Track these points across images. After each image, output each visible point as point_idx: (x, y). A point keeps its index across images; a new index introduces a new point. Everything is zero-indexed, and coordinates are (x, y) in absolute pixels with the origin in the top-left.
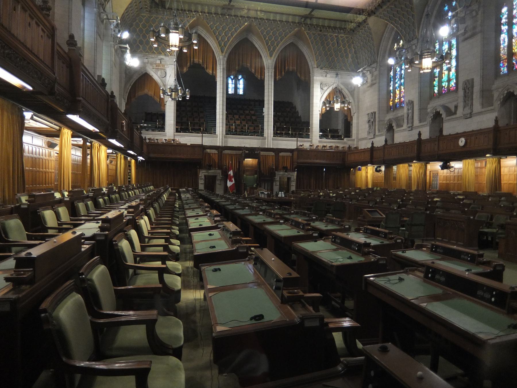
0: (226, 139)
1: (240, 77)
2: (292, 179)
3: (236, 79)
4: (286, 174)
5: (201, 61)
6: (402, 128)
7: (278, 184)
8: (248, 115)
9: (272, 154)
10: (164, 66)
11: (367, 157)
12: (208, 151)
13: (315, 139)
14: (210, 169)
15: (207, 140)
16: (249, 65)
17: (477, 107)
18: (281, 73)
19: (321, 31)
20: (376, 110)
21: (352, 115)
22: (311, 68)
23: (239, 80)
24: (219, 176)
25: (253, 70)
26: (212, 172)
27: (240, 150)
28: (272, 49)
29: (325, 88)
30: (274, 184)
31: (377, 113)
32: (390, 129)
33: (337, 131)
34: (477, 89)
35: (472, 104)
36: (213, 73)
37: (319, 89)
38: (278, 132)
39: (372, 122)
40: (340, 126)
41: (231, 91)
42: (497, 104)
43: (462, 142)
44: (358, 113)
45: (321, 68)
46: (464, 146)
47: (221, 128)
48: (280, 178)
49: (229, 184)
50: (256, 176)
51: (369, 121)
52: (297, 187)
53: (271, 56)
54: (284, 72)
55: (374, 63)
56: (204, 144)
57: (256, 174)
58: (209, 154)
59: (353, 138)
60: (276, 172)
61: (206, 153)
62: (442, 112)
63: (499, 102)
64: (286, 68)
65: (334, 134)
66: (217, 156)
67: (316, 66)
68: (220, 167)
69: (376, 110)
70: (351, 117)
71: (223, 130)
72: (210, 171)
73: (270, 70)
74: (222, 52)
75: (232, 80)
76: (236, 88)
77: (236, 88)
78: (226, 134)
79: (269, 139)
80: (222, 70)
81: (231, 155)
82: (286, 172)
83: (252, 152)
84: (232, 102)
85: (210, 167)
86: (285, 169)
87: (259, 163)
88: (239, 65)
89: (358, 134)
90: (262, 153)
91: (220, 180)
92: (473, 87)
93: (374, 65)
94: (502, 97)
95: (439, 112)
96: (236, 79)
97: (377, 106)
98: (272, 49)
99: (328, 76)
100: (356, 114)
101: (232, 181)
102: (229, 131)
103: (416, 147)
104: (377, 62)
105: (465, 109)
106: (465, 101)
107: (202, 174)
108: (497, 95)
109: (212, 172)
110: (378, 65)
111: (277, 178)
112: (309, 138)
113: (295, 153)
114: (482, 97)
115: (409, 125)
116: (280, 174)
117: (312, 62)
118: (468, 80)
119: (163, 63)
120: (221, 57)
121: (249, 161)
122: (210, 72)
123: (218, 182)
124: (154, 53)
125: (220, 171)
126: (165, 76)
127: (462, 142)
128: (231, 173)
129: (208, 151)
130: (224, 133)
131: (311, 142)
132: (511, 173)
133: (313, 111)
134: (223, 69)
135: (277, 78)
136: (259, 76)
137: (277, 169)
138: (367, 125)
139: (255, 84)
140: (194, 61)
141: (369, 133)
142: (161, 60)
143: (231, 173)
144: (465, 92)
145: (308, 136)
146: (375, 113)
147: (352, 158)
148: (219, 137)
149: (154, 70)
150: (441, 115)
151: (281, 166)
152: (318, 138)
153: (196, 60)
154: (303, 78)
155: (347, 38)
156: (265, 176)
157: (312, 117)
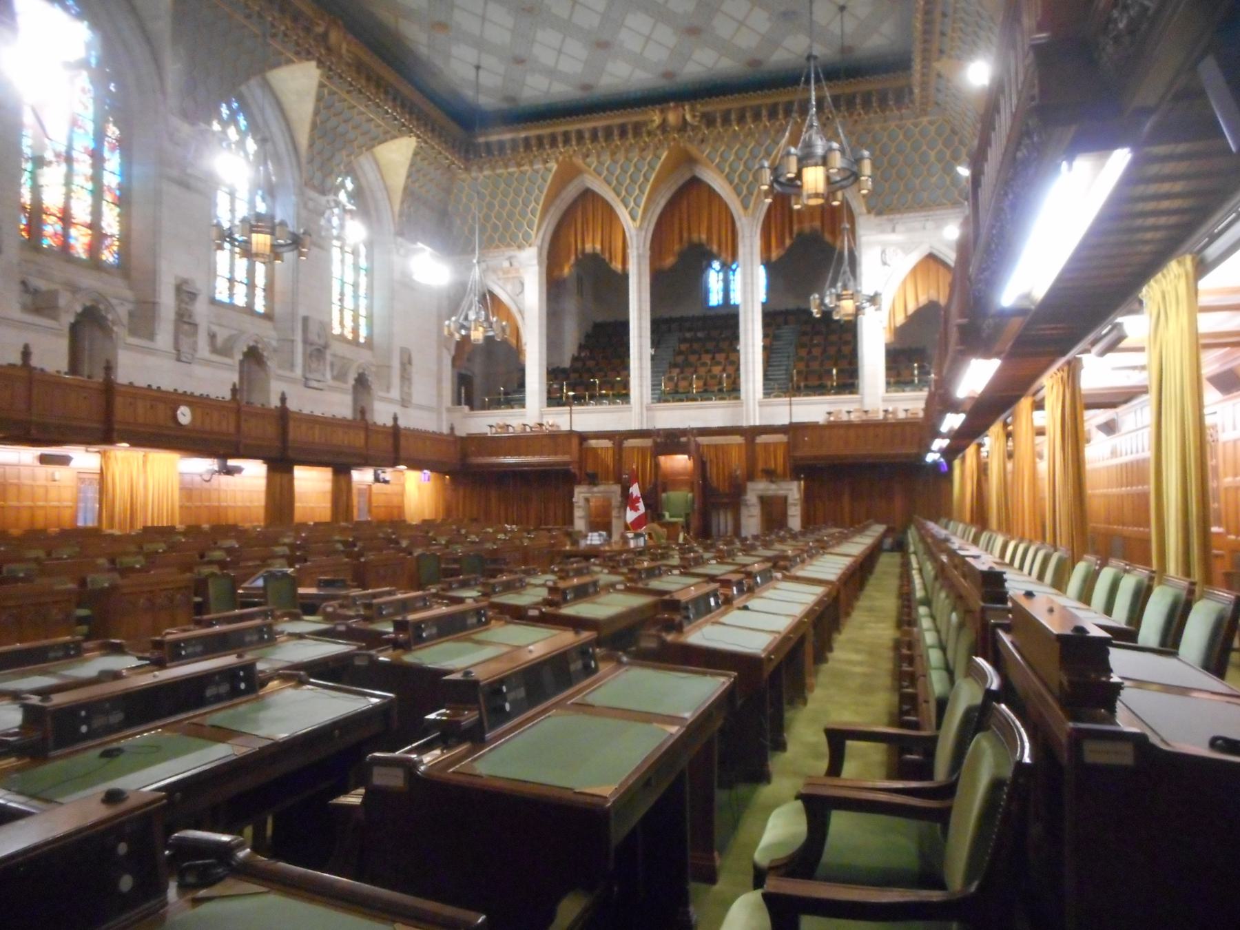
2: (790, 501)
4: (773, 486)
5: (598, 247)
9: (738, 439)
10: (517, 270)
12: (593, 443)
13: (876, 395)
14: (595, 485)
15: (591, 418)
16: (704, 237)
18: (781, 242)
24: (616, 499)
25: (715, 248)
28: (745, 192)
30: (744, 512)
38: (776, 384)
45: (880, 213)
49: (631, 516)
50: (690, 495)
54: (791, 237)
56: (578, 427)
58: (595, 450)
60: (750, 485)
64: (795, 228)
66: (611, 452)
67: (864, 210)
68: (618, 480)
72: (595, 489)
74: (633, 218)
79: (756, 404)
81: (642, 450)
82: (772, 482)
83: (671, 441)
85: (592, 480)
86: (770, 475)
87: (701, 466)
98: (745, 192)
99: (899, 228)
101: (636, 509)
102: (661, 397)
107: (580, 494)
116: (756, 489)
119: (515, 264)
120: (633, 232)
121: (680, 462)
122: (616, 266)
123: (614, 513)
124: (498, 247)
126: (522, 291)
128: (635, 490)
129: (593, 443)
131: (861, 401)
137: (751, 476)
140: (583, 249)
142: (510, 259)
143: (635, 490)
148: (640, 408)
149: (501, 283)
151: (760, 466)
153: (588, 248)
155: (931, 123)
156: (715, 496)
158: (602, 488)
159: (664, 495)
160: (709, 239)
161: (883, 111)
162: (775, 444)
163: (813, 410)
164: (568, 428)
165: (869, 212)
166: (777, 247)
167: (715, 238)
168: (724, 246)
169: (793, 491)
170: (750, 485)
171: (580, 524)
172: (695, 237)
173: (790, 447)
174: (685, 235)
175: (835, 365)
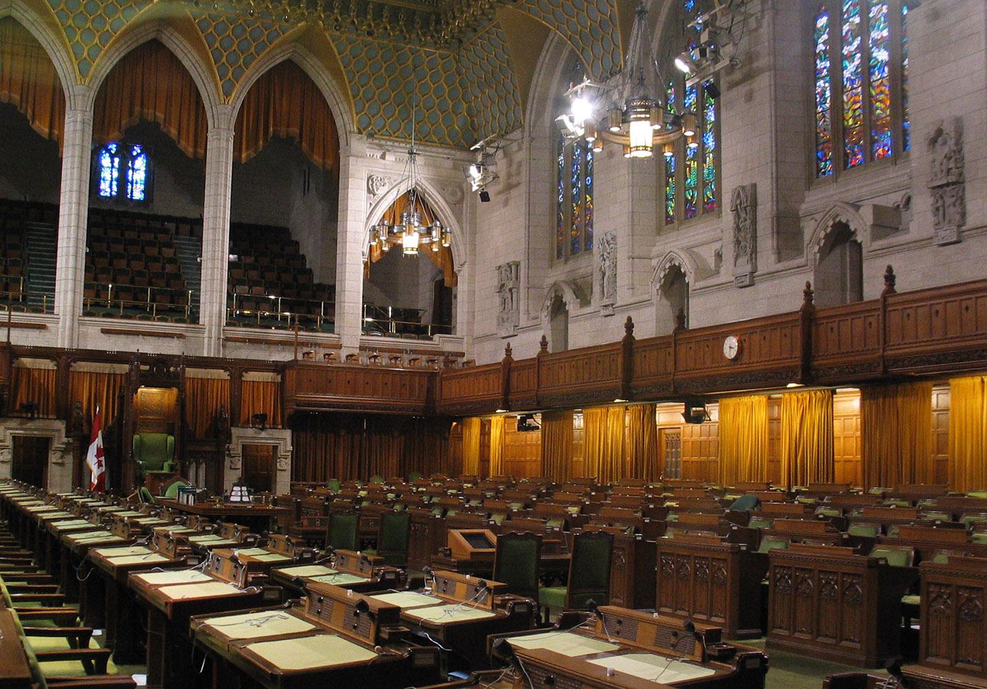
0: (83, 329)
1: (137, 150)
2: (281, 452)
3: (125, 157)
4: (263, 434)
6: (587, 310)
7: (239, 465)
8: (156, 260)
9: (222, 374)
11: (494, 388)
12: (27, 362)
14: (32, 419)
16: (161, 116)
17: (767, 260)
19: (370, 34)
20: (520, 257)
21: (456, 269)
22: (341, 132)
23: (135, 158)
25: (173, 132)
26: (35, 428)
27: (126, 362)
29: (381, 191)
31: (522, 265)
32: (558, 309)
33: (413, 314)
34: (766, 209)
35: (754, 251)
36: (51, 133)
37: (364, 193)
39: (510, 290)
40: (424, 300)
41: (107, 188)
42: (812, 252)
43: (731, 346)
44: (473, 263)
46: (735, 359)
47: (70, 295)
48: (244, 447)
50: (171, 439)
51: (503, 285)
52: (297, 474)
53: (227, 94)
54: (265, 140)
55: (514, 129)
57: (171, 434)
58: (29, 371)
59: (459, 334)
60: (235, 431)
61: (18, 369)
62: (687, 267)
63: (816, 248)
65: (409, 324)
69: (520, 257)
70: (454, 276)
71: (74, 300)
72: (29, 425)
73: (224, 134)
75: (112, 156)
76: (123, 181)
77: (123, 181)
78: (86, 314)
80: (79, 127)
82: (263, 429)
83: (160, 370)
84: (106, 218)
85: (30, 411)
86: (260, 421)
87: (181, 401)
88: (131, 115)
89: (471, 323)
90: (191, 372)
91: (64, 452)
92: (754, 205)
93: (516, 135)
94: (822, 234)
95: (679, 268)
96: (125, 157)
97: (523, 246)
99: (390, 157)
100: (466, 266)
103: (620, 360)
104: (522, 126)
105: (740, 260)
106: (738, 242)
108: (813, 232)
109: (35, 428)
110: (526, 134)
111: (236, 447)
112: (332, 331)
113: (291, 375)
114: (778, 233)
115: (606, 301)
116: (242, 435)
117: (345, 118)
118: (743, 188)
121: (149, 395)
122: (42, 128)
123: (53, 458)
125: (60, 425)
127: (731, 346)
129: (27, 362)
130: (80, 311)
132: (849, 433)
133: (344, 254)
134: (83, 122)
135: (244, 155)
136: (191, 150)
137: (235, 421)
138: (497, 300)
139: (181, 170)
141: (502, 321)
144: (738, 216)
145: (329, 325)
146: (517, 265)
147: (453, 391)
150: (684, 275)
151: (247, 411)
152: (360, 332)
154: (317, 159)
157: (344, 273)
158: (38, 424)
159: (136, 437)
160: (167, 120)
161: (409, 31)
162: (266, 383)
163: (277, 346)
164: (5, 340)
165: (360, 132)
166: (247, 149)
167: (174, 121)
168: (184, 132)
169: (284, 439)
170: (235, 431)
171: (232, 475)
172: (149, 114)
173: (281, 385)
174: (137, 109)
175: (114, 281)
